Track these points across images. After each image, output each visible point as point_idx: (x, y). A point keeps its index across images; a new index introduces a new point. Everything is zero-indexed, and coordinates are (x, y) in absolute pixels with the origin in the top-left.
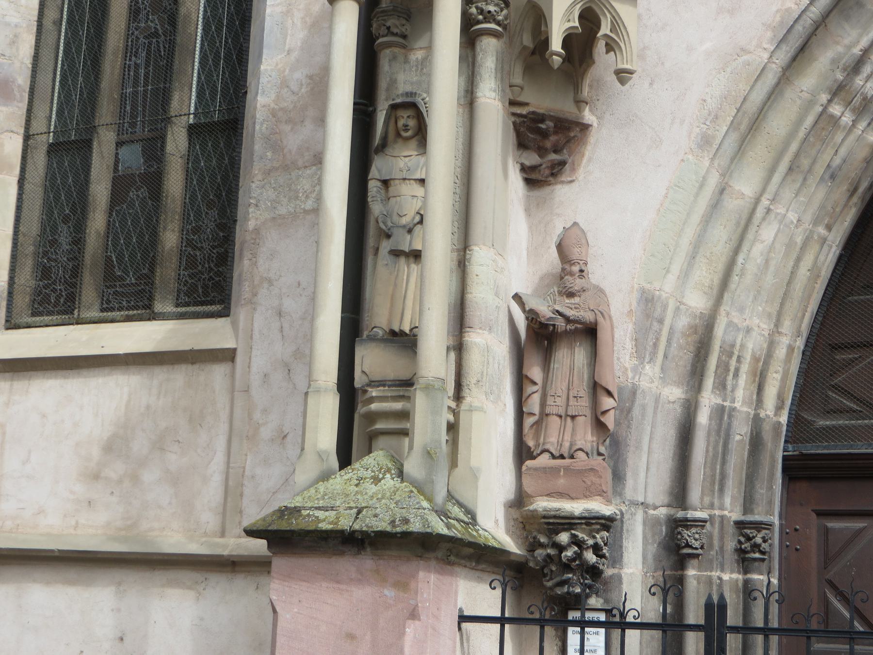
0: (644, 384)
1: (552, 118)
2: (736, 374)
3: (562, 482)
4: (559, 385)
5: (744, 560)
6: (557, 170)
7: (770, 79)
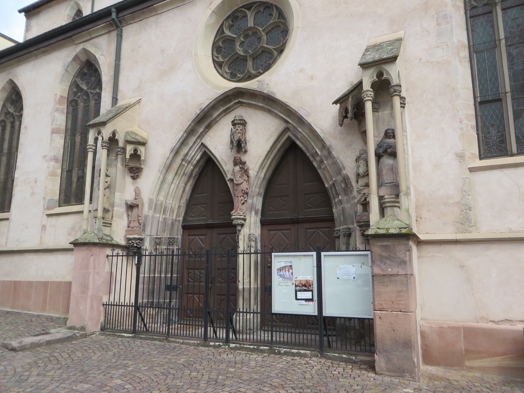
0: (149, 214)
1: (135, 167)
2: (168, 212)
3: (131, 232)
4: (133, 216)
5: (169, 244)
6: (138, 177)
7: (170, 159)
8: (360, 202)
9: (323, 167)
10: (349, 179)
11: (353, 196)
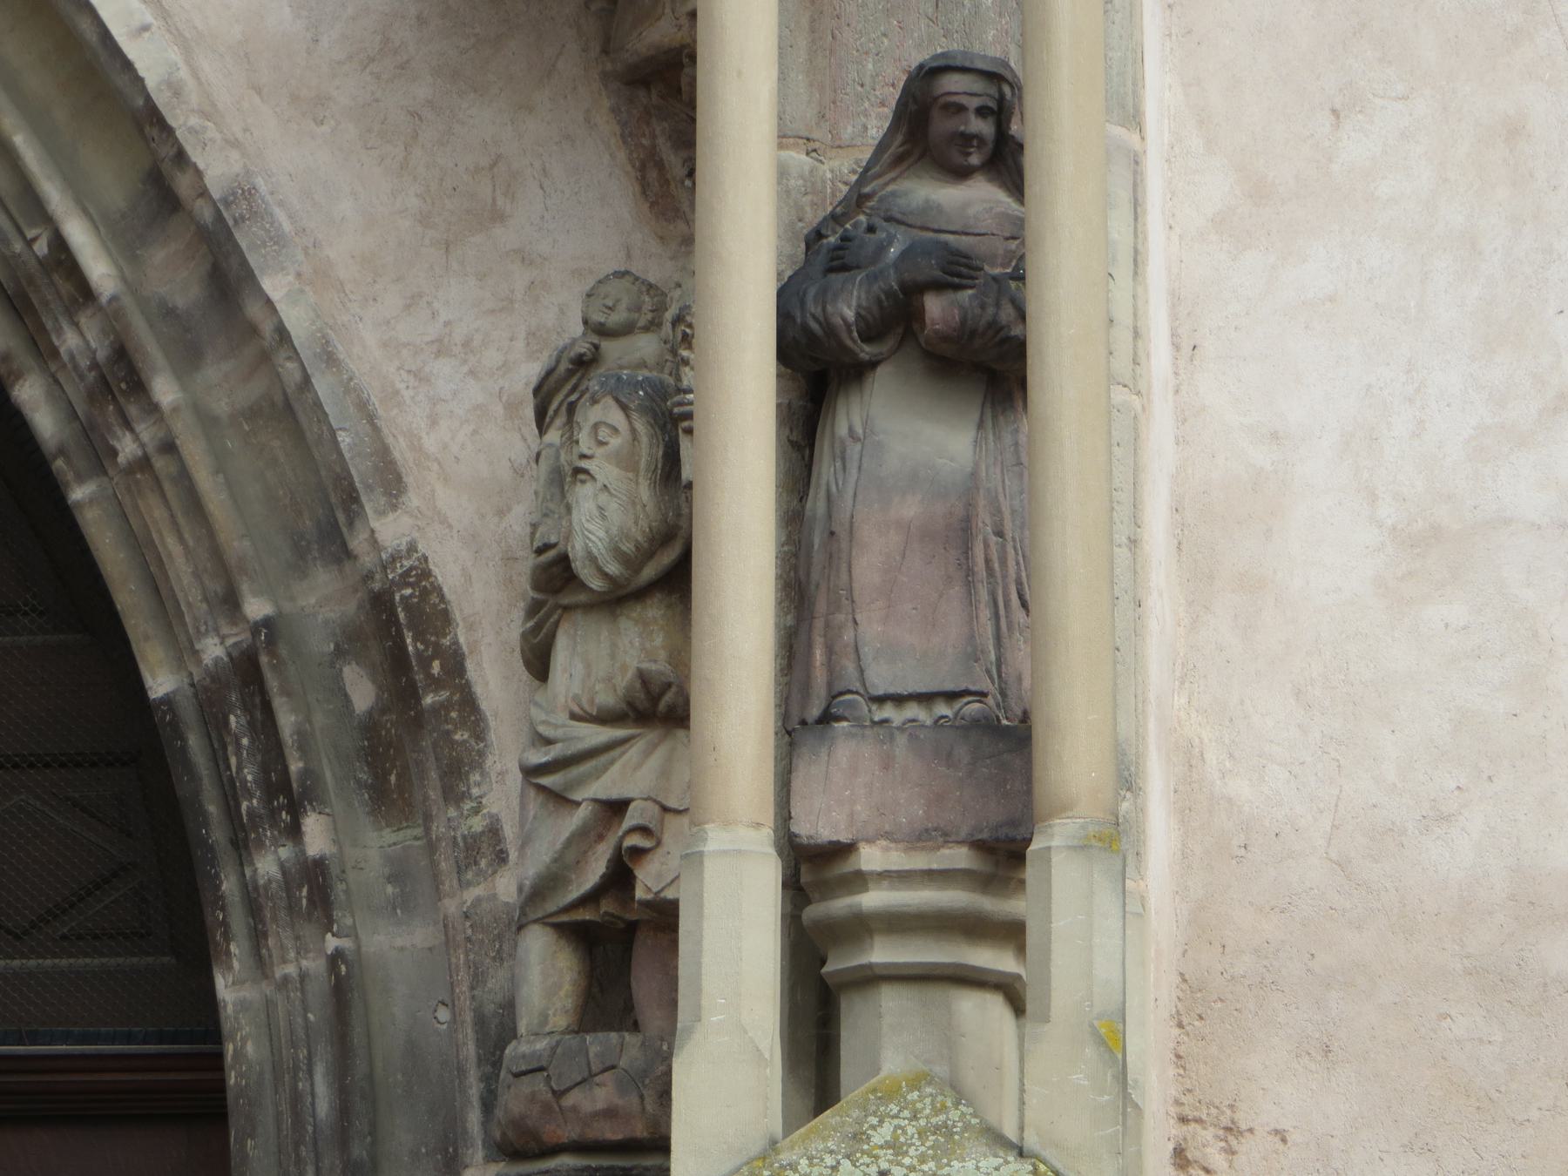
8: (551, 906)
9: (127, 448)
10: (445, 617)
11: (477, 824)
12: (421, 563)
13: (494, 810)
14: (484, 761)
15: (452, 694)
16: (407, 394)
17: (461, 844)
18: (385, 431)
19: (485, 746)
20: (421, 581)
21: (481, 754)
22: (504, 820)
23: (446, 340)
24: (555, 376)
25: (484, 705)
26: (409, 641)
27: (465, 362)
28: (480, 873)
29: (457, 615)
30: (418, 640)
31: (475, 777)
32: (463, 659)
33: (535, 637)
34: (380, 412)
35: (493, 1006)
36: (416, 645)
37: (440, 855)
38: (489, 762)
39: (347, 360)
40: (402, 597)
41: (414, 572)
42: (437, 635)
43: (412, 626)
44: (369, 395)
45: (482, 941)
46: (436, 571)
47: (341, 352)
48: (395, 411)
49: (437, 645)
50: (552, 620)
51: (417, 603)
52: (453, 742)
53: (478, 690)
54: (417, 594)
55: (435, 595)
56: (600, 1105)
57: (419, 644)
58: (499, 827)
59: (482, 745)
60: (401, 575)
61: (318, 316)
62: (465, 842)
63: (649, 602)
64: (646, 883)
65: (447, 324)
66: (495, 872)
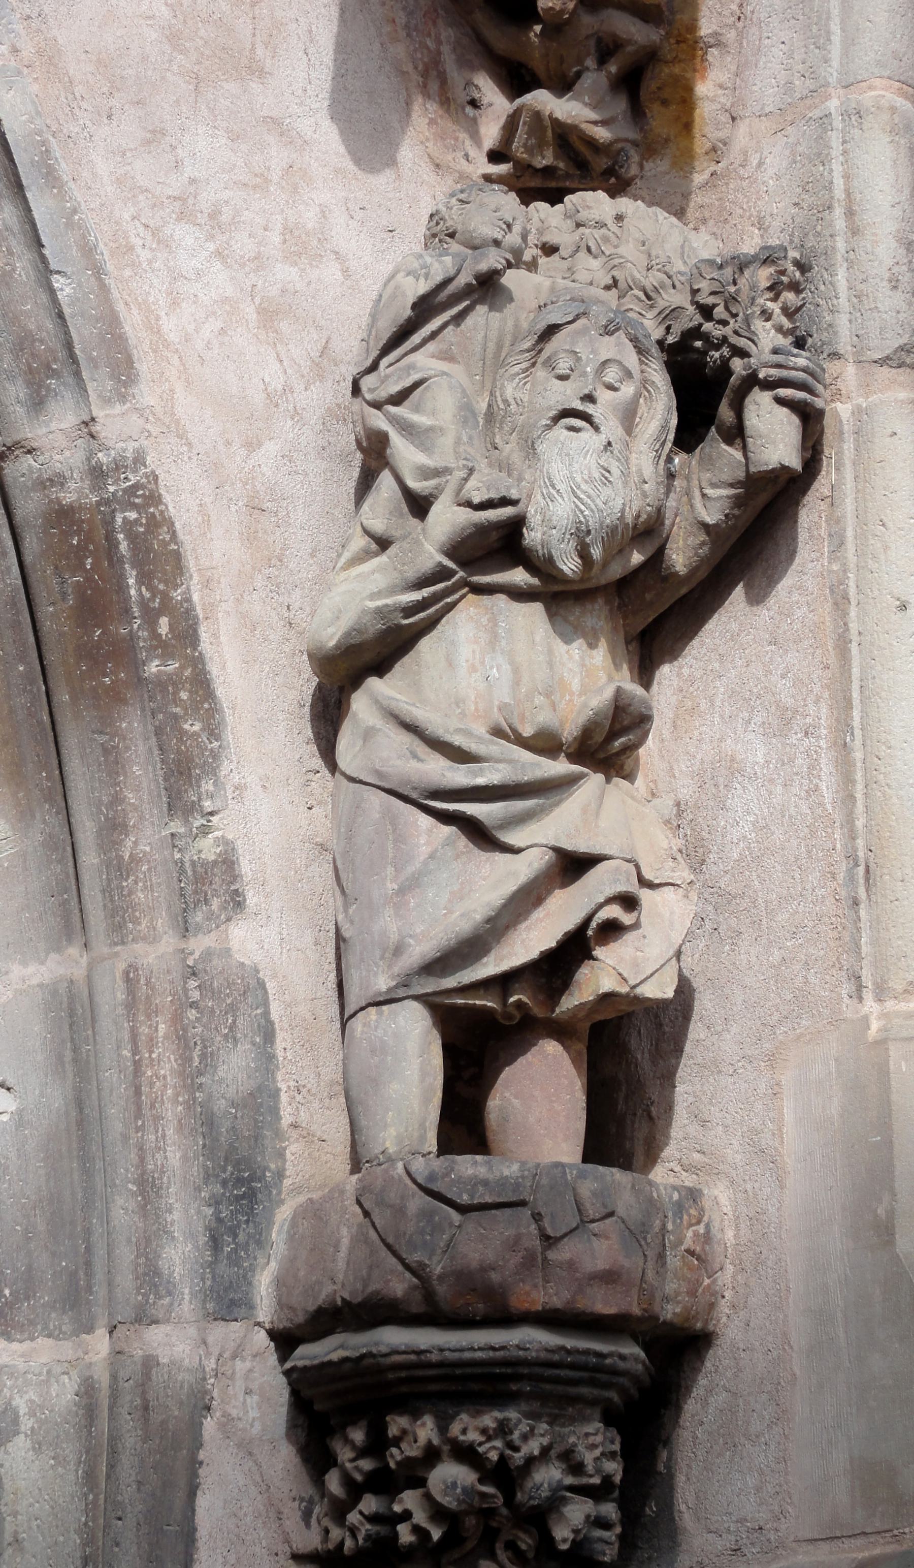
8: (450, 982)
12: (149, 482)
13: (230, 837)
14: (218, 767)
15: (182, 667)
16: (144, 255)
17: (190, 873)
18: (115, 294)
19: (220, 746)
20: (150, 506)
21: (215, 755)
22: (240, 852)
23: (191, 201)
24: (451, 288)
25: (220, 692)
26: (131, 581)
27: (211, 237)
28: (210, 917)
29: (191, 563)
30: (143, 584)
31: (207, 786)
32: (196, 624)
33: (406, 617)
34: (110, 267)
35: (223, 1101)
36: (140, 589)
37: (136, 883)
38: (225, 767)
39: (71, 184)
40: (124, 518)
41: (141, 492)
42: (166, 583)
43: (137, 564)
44: (96, 239)
45: (212, 1011)
46: (167, 498)
47: (64, 169)
48: (128, 272)
49: (165, 597)
50: (449, 600)
51: (143, 533)
52: (182, 732)
53: (214, 669)
54: (144, 521)
55: (165, 529)
56: (601, 1264)
57: (143, 589)
58: (235, 858)
59: (216, 744)
60: (125, 491)
61: (38, 113)
62: (194, 872)
63: (589, 606)
64: (620, 971)
65: (192, 181)
66: (229, 920)
